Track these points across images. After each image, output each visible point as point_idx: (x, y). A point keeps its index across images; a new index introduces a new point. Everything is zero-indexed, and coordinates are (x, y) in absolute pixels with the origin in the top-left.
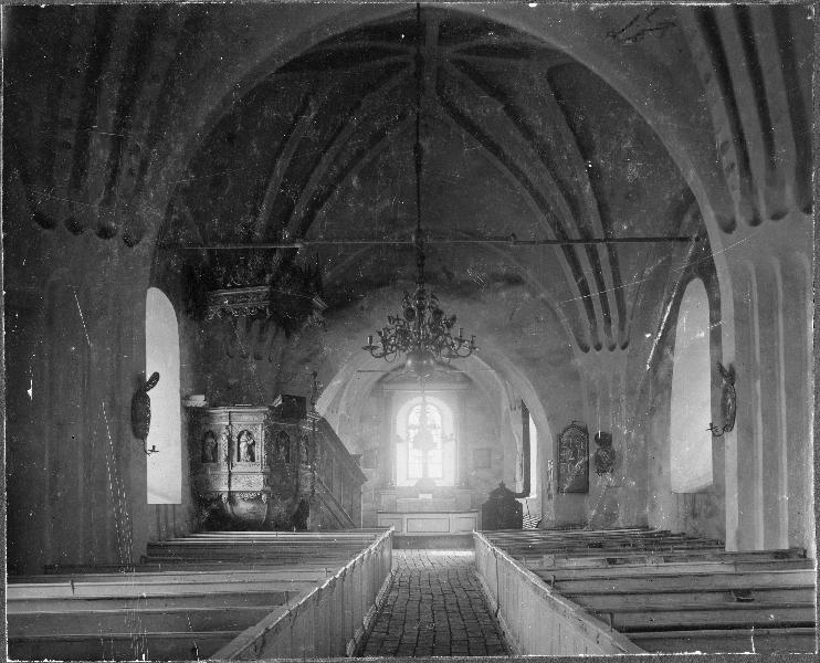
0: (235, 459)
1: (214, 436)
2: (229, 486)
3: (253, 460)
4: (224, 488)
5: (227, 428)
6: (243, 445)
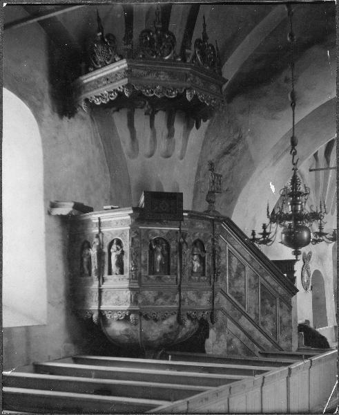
0: (106, 271)
2: (100, 304)
3: (122, 272)
5: (98, 236)
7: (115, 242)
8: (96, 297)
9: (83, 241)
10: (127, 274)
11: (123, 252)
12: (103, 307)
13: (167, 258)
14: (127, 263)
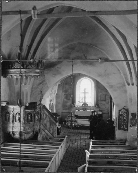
0: (15, 121)
1: (9, 113)
2: (13, 130)
4: (11, 130)
5: (12, 112)
7: (18, 113)
9: (6, 111)
12: (14, 131)
13: (31, 118)
14: (22, 120)
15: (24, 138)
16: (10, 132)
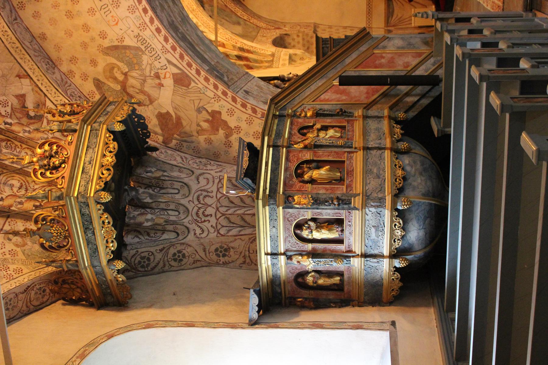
2: (383, 256)
3: (340, 222)
6: (317, 235)
7: (298, 232)
8: (372, 262)
9: (294, 284)
10: (343, 214)
11: (314, 220)
12: (386, 252)
13: (319, 164)
14: (327, 213)
15: (425, 195)
16: (397, 269)
